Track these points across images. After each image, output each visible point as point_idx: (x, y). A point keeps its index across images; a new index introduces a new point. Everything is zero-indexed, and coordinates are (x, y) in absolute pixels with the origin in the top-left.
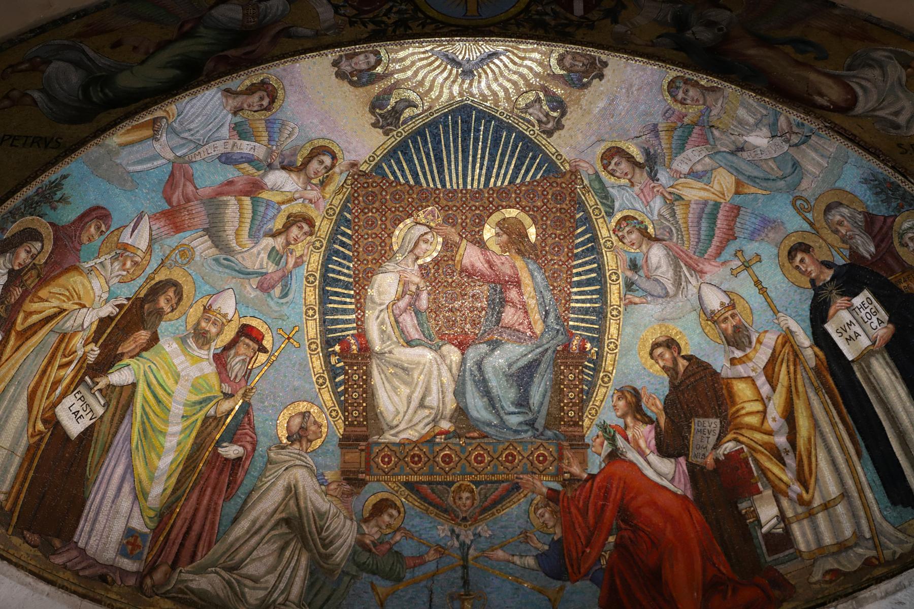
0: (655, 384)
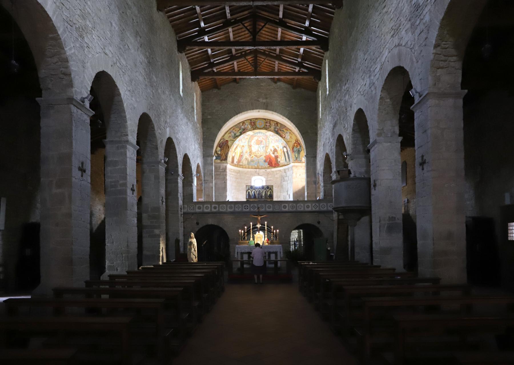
0: (273, 150)
